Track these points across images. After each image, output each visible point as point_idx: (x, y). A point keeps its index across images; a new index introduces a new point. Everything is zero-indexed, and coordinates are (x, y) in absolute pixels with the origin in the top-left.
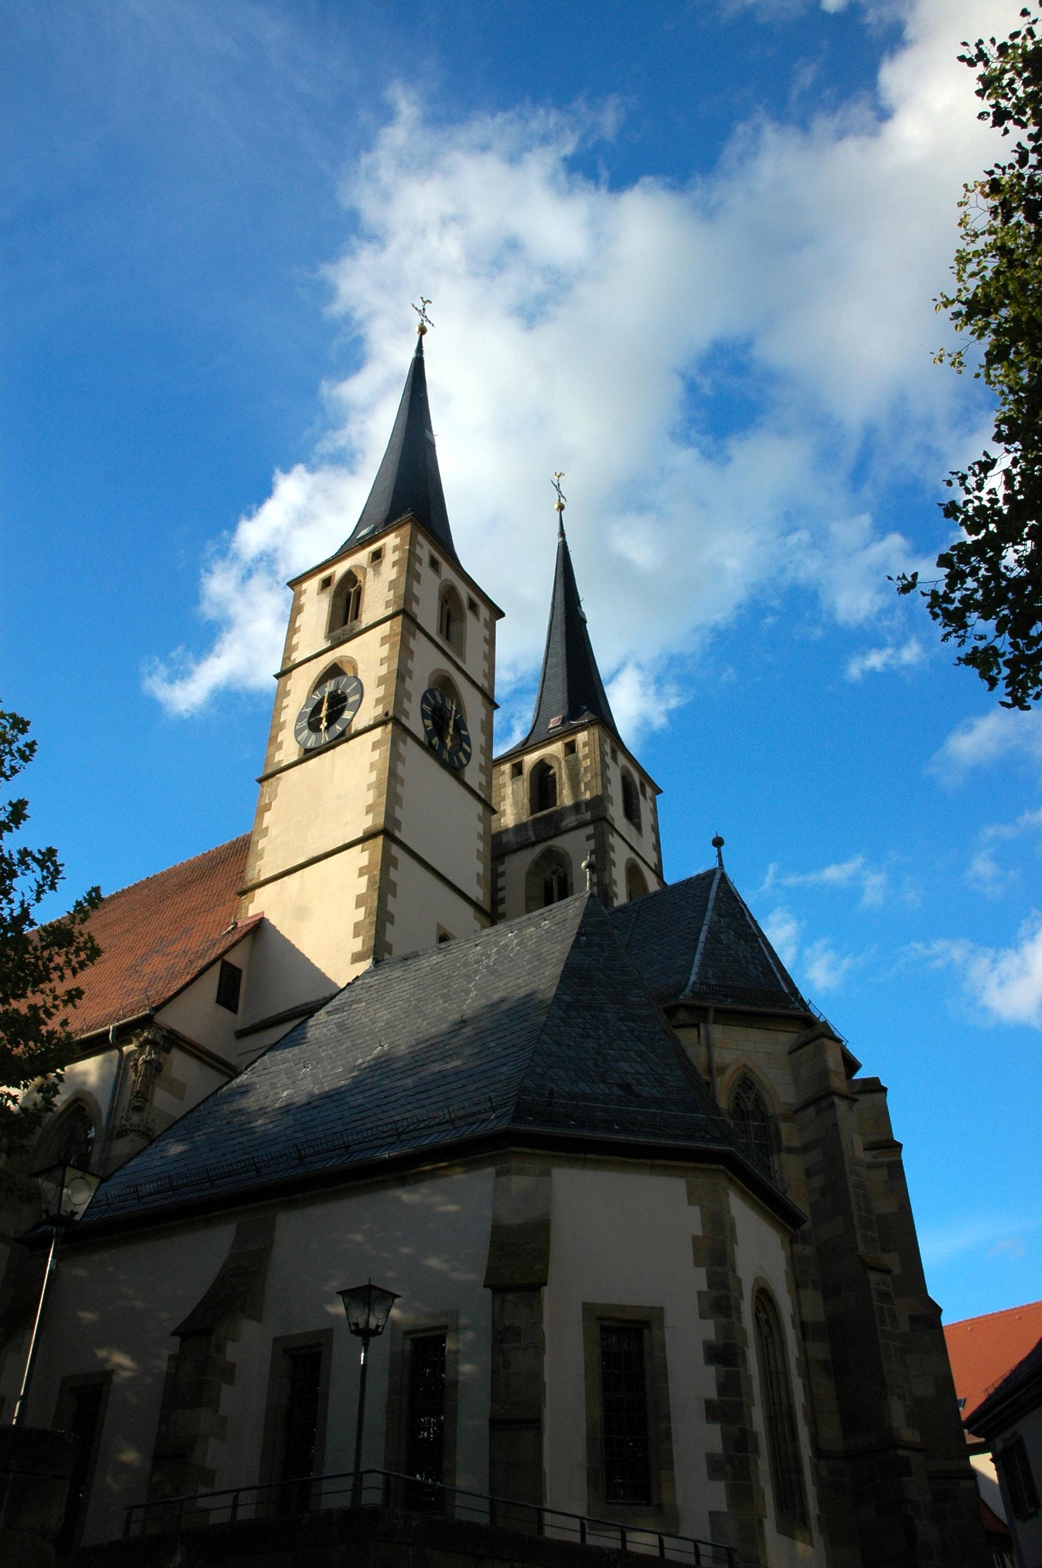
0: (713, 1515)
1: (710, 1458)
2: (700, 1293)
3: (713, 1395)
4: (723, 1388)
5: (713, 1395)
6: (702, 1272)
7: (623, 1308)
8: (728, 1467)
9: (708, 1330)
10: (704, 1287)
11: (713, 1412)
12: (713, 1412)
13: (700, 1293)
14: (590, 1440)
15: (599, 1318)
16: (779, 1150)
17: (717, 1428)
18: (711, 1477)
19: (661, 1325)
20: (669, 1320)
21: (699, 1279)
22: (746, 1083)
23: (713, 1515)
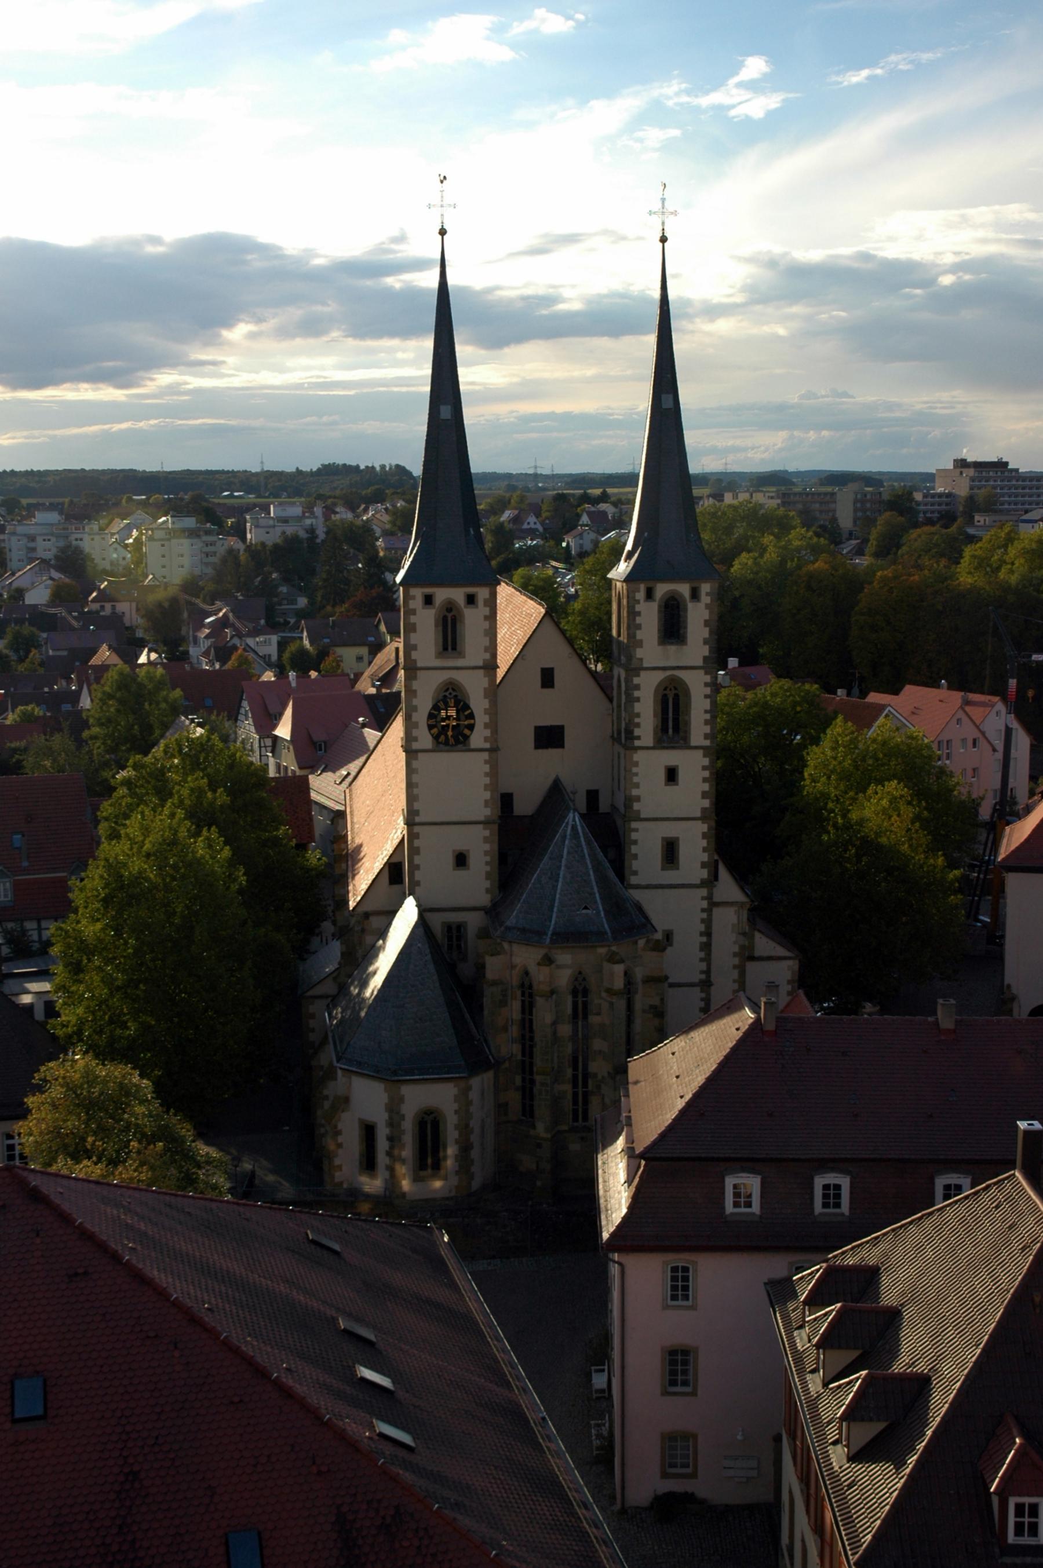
21: (386, 1116)
22: (527, 973)
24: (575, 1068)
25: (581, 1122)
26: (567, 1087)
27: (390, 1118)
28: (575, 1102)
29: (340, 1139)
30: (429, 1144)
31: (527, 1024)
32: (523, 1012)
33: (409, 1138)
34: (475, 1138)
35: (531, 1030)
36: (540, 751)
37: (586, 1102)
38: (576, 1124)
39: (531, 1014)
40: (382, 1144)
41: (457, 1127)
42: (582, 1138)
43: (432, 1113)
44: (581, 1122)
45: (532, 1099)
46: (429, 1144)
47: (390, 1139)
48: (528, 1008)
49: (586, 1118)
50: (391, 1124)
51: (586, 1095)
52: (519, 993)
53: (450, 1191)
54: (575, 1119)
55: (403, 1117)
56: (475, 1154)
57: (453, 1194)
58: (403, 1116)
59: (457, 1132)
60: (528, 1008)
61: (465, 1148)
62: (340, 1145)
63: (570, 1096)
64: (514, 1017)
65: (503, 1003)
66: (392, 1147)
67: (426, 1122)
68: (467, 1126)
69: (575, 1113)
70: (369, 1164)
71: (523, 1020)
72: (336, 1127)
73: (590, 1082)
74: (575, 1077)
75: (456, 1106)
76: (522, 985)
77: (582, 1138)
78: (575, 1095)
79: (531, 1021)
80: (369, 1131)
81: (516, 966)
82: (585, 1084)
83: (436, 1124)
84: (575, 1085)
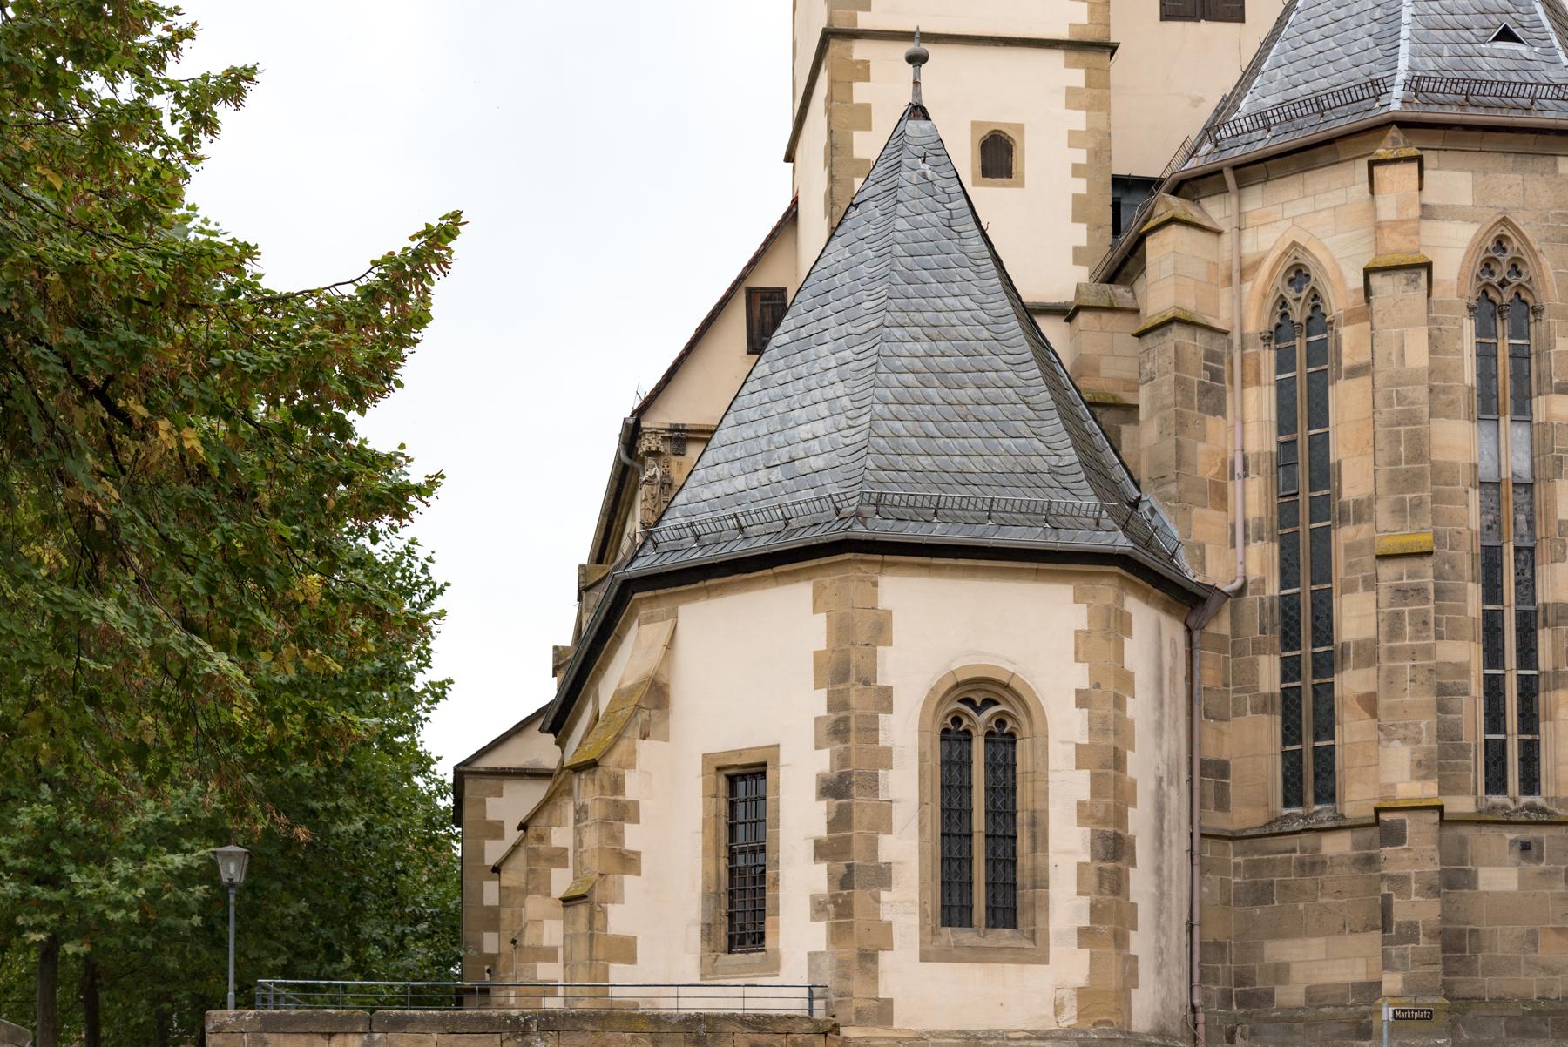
0: (812, 956)
1: (813, 897)
2: (817, 719)
3: (822, 832)
4: (832, 825)
5: (822, 832)
6: (823, 693)
7: (739, 753)
8: (831, 907)
9: (823, 762)
10: (823, 712)
11: (822, 851)
12: (822, 851)
13: (817, 719)
14: (706, 896)
15: (719, 769)
16: (1338, 377)
17: (823, 867)
18: (813, 919)
19: (776, 767)
20: (784, 757)
21: (817, 703)
23: (812, 956)
24: (1492, 591)
25: (1513, 797)
26: (1466, 652)
27: (837, 703)
28: (1494, 720)
29: (632, 837)
30: (979, 822)
31: (1303, 465)
32: (1285, 421)
33: (906, 785)
34: (1139, 822)
35: (1323, 473)
36: (1176, 27)
37: (1530, 719)
38: (1497, 799)
39: (1319, 414)
40: (798, 815)
41: (1082, 756)
42: (1526, 847)
43: (989, 702)
44: (1513, 797)
45: (1326, 727)
46: (979, 822)
47: (834, 788)
48: (1303, 407)
49: (1530, 783)
50: (837, 729)
51: (1528, 690)
52: (1268, 358)
53: (1058, 1009)
54: (1496, 783)
55: (885, 699)
56: (1140, 883)
57: (1069, 1019)
58: (887, 693)
59: (1085, 775)
60: (1303, 407)
61: (1113, 848)
62: (629, 862)
63: (1476, 689)
64: (1253, 446)
65: (1212, 397)
66: (839, 821)
67: (967, 736)
68: (1119, 762)
69: (1495, 756)
70: (741, 916)
71: (1287, 448)
72: (617, 785)
73: (1545, 639)
74: (1491, 628)
75: (1080, 676)
76: (1280, 332)
77: (1526, 847)
78: (1494, 689)
79: (1320, 445)
80: (743, 785)
81: (1256, 265)
82: (1527, 654)
83: (1003, 740)
84: (1493, 654)
